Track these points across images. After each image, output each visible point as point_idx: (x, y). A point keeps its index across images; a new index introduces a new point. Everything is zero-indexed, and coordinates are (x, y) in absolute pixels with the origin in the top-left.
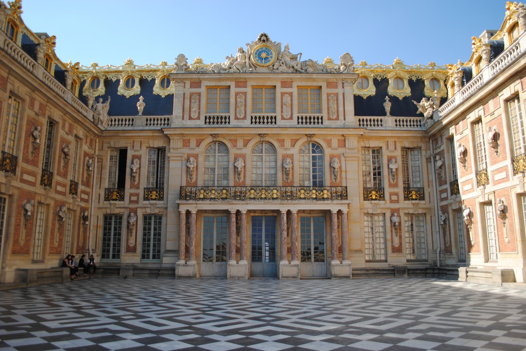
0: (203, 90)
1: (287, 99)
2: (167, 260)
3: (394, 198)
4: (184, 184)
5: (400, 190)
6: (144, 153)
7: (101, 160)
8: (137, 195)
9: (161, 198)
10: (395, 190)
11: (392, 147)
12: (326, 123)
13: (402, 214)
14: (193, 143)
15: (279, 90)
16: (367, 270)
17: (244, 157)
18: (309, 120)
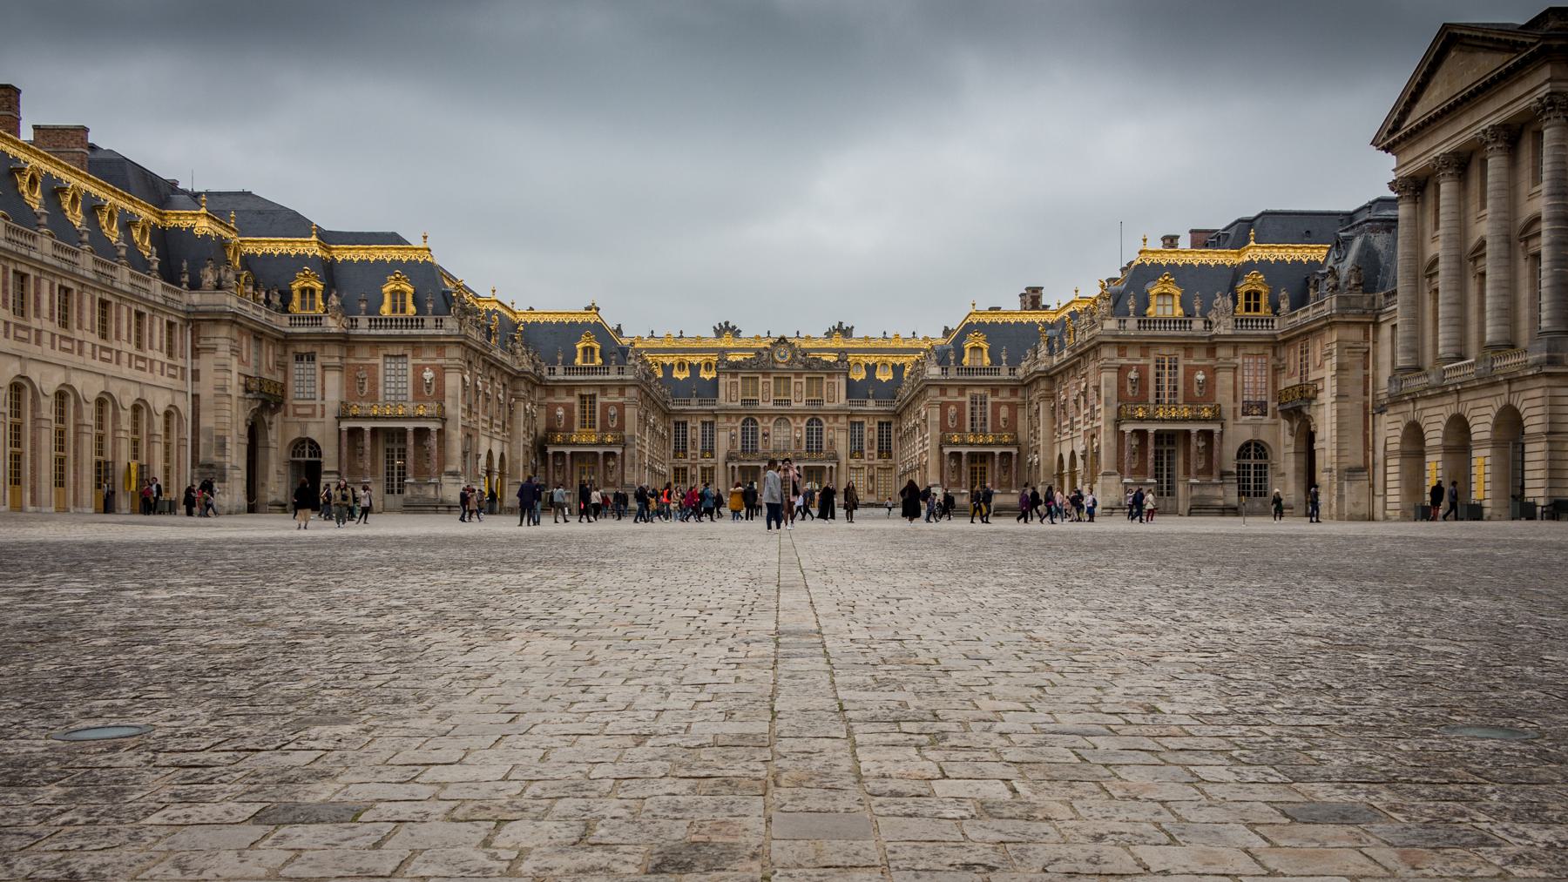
0: (739, 380)
1: (799, 387)
5: (875, 451)
6: (699, 425)
15: (793, 380)
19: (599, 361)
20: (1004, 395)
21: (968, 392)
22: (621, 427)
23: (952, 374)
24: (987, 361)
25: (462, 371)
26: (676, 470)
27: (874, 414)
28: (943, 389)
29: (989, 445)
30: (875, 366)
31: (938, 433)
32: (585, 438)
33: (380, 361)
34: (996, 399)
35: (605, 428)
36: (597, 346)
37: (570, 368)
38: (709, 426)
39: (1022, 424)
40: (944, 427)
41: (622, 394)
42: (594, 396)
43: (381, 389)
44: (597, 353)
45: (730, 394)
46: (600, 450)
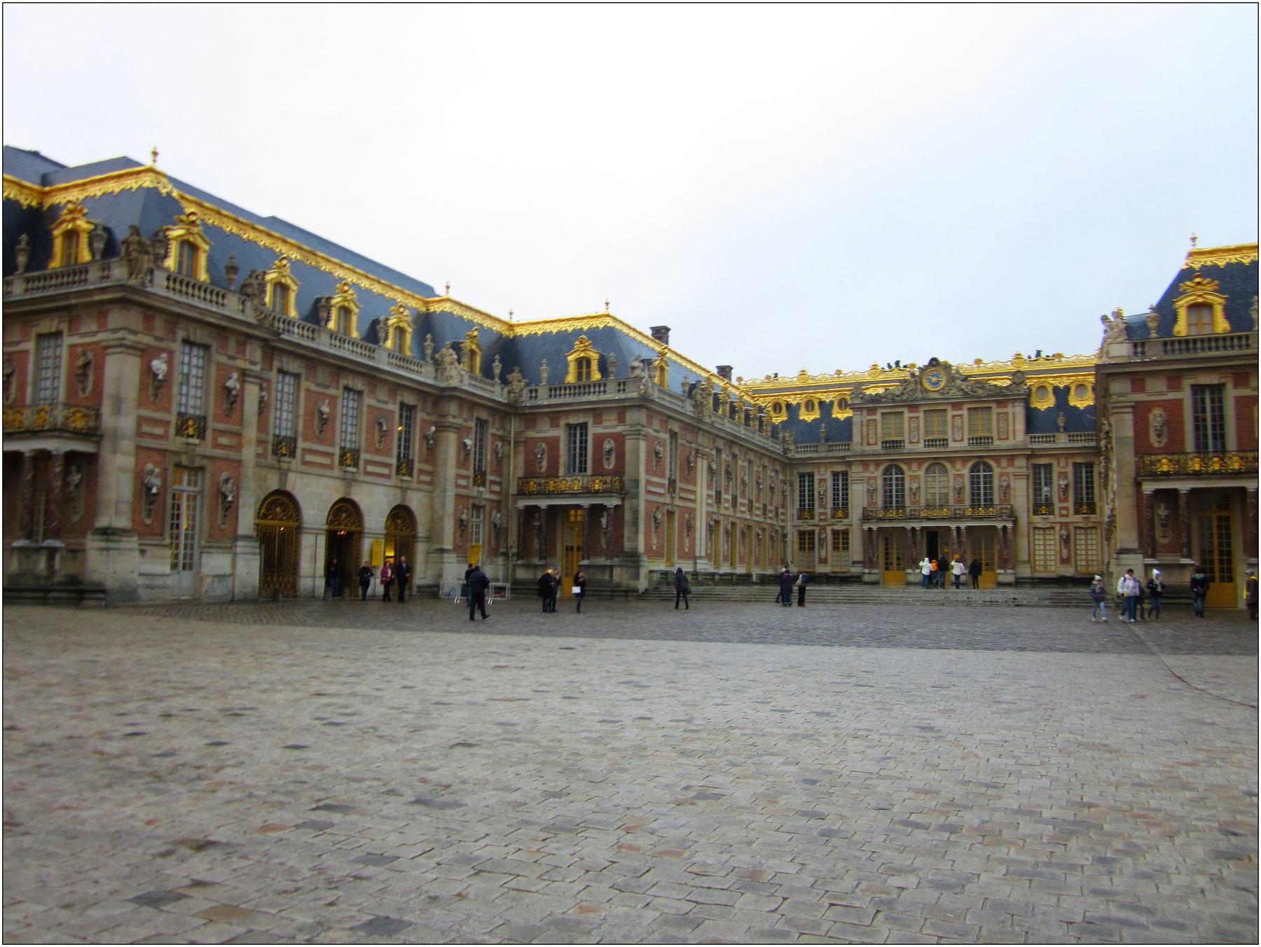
0: (878, 417)
1: (958, 422)
2: (856, 570)
3: (1064, 512)
4: (866, 505)
6: (829, 477)
7: (792, 484)
8: (825, 514)
9: (846, 516)
10: (1065, 505)
11: (1062, 463)
12: (997, 443)
13: (1071, 528)
14: (872, 468)
15: (950, 413)
16: (1032, 578)
17: (917, 477)
18: (978, 440)
19: (596, 376)
21: (1187, 383)
22: (620, 470)
24: (1222, 325)
25: (146, 353)
26: (802, 534)
27: (1067, 454)
30: (1067, 388)
31: (1129, 456)
32: (573, 489)
33: (30, 346)
35: (599, 471)
36: (594, 356)
38: (842, 478)
40: (1142, 447)
41: (621, 420)
42: (584, 426)
43: (29, 390)
44: (594, 365)
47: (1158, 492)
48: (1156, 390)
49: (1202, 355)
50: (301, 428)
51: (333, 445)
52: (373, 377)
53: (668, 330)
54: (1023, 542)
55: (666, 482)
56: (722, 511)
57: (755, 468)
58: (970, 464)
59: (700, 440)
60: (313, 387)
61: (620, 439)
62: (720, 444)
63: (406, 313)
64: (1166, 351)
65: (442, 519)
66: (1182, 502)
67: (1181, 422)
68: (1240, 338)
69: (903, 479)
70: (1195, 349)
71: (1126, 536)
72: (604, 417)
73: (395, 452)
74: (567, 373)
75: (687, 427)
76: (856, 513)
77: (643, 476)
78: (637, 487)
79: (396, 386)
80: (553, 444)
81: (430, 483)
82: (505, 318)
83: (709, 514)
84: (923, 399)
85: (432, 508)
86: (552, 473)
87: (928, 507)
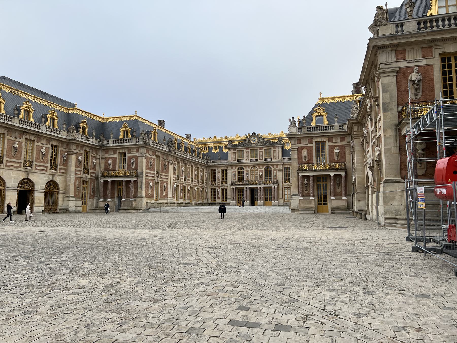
1: (261, 153)
2: (228, 201)
6: (221, 171)
7: (209, 173)
9: (226, 184)
12: (273, 160)
14: (234, 168)
15: (258, 150)
17: (248, 171)
20: (337, 141)
21: (314, 141)
22: (137, 168)
23: (305, 130)
24: (326, 122)
26: (212, 189)
28: (299, 140)
29: (327, 170)
34: (331, 144)
35: (130, 168)
36: (129, 129)
37: (116, 140)
39: (348, 157)
40: (300, 161)
41: (137, 151)
42: (125, 153)
44: (129, 133)
45: (233, 158)
46: (124, 179)
47: (304, 176)
48: (305, 143)
49: (319, 132)
50: (5, 153)
51: (21, 159)
52: (39, 135)
53: (164, 122)
54: (281, 192)
55: (155, 173)
56: (180, 182)
57: (194, 168)
58: (265, 167)
59: (170, 159)
60: (11, 138)
61: (137, 158)
62: (179, 160)
63: (55, 113)
64: (308, 131)
65: (69, 185)
66: (311, 179)
67: (312, 153)
68: (331, 126)
69: (244, 172)
70: (317, 130)
71: (295, 191)
72: (132, 151)
73: (49, 162)
74: (120, 135)
75: (164, 154)
76: (229, 183)
77: (144, 171)
78: (142, 174)
79: (49, 139)
80: (114, 159)
81: (65, 173)
82: (102, 116)
83: (174, 183)
84: (250, 146)
85: (66, 181)
86: (114, 170)
87: (251, 181)
